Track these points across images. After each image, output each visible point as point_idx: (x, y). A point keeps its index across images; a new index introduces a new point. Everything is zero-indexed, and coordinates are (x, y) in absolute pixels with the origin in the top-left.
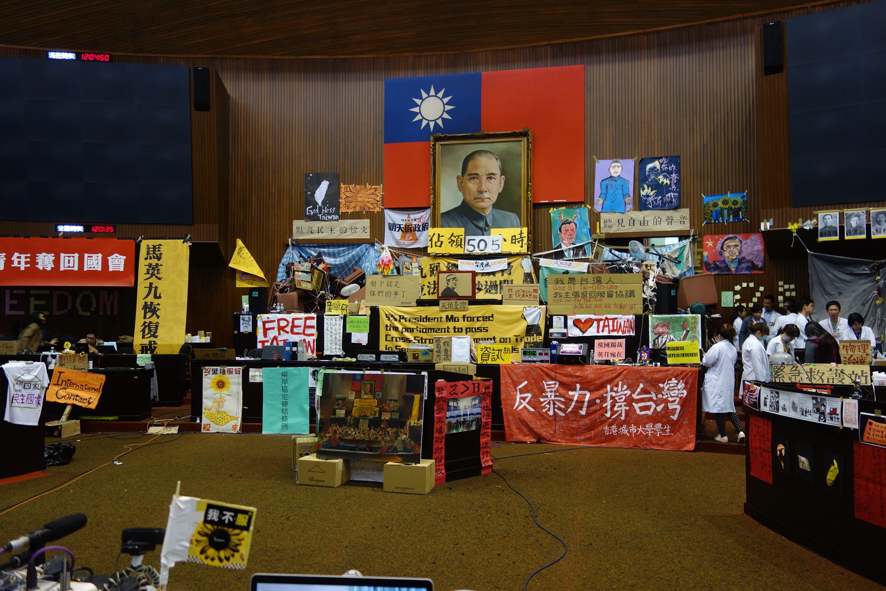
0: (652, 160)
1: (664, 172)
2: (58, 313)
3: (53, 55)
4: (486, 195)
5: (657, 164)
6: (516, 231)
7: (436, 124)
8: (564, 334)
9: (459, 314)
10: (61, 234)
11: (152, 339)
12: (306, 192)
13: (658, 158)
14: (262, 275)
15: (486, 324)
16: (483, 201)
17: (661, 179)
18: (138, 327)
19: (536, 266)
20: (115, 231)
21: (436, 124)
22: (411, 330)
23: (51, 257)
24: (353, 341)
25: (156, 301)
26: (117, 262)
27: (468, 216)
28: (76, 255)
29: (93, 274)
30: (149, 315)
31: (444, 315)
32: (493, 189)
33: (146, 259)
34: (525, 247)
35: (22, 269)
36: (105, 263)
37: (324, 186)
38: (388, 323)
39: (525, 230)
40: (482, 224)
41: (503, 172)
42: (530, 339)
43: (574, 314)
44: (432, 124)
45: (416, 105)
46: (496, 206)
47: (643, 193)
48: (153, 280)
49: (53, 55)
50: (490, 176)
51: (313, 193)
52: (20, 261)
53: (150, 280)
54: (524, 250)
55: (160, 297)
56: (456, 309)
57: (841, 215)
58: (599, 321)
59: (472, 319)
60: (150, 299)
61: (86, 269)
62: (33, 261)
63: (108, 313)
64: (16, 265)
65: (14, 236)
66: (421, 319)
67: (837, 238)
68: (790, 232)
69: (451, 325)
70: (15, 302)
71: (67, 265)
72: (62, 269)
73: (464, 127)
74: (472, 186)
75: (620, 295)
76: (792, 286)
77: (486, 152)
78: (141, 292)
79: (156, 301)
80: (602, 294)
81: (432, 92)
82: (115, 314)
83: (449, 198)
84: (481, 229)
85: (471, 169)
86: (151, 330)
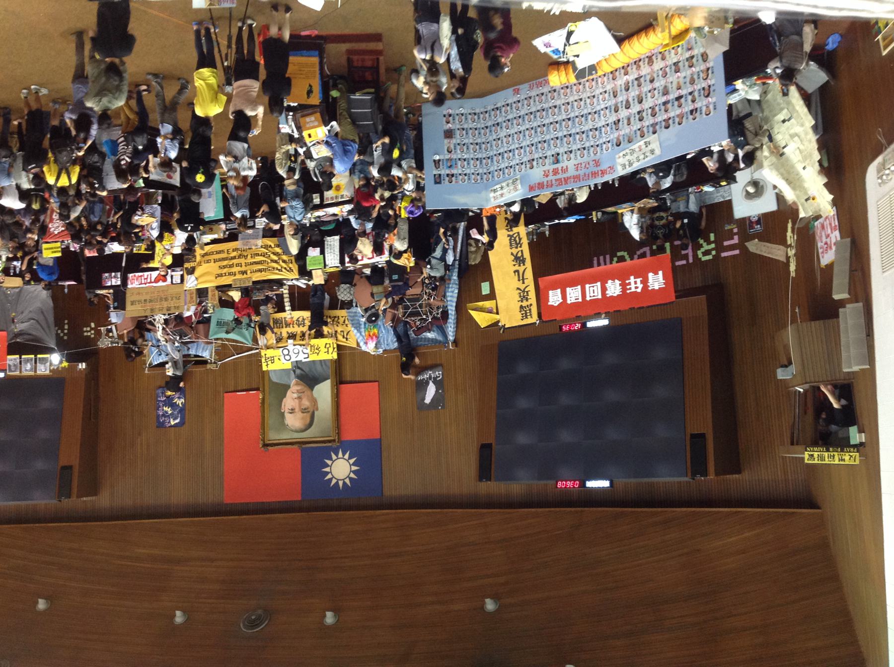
0: (176, 425)
1: (168, 416)
2: (645, 249)
3: (606, 484)
4: (295, 395)
5: (173, 423)
6: (272, 367)
7: (337, 455)
8: (173, 271)
9: (238, 276)
10: (603, 316)
11: (511, 233)
12: (443, 391)
13: (171, 426)
14: (472, 313)
15: (220, 271)
16: (298, 391)
17: (169, 410)
18: (525, 242)
19: (255, 340)
20: (561, 327)
21: (337, 455)
22: (273, 261)
23: (609, 293)
24: (318, 250)
25: (517, 268)
26: (554, 298)
27: (308, 376)
28: (588, 298)
29: (573, 284)
30: (520, 254)
31: (249, 275)
32: (290, 401)
33: (531, 305)
34: (263, 354)
35: (632, 277)
36: (564, 296)
37: (428, 400)
38: (291, 265)
39: (265, 368)
40: (298, 371)
41: (282, 415)
42: (192, 264)
43: (168, 285)
44: (340, 455)
45: (354, 472)
46: (287, 387)
47: (183, 400)
48: (522, 287)
49: (606, 484)
50: (292, 411)
51: (437, 391)
52: (635, 285)
53: (524, 286)
54: (263, 353)
55: (515, 272)
56: (240, 280)
57: (35, 371)
58: (151, 282)
59: (230, 274)
60: (521, 269)
61: (579, 287)
62: (624, 286)
63: (601, 258)
64: (639, 280)
65: (643, 307)
66: (265, 270)
67: (39, 356)
68: (67, 361)
69: (243, 268)
70: (683, 252)
71: (595, 288)
72: (599, 284)
73: (314, 455)
74: (306, 403)
75: (139, 301)
76: (85, 334)
77: (297, 431)
78: (529, 274)
79: (517, 268)
80: (151, 301)
81: (341, 483)
82: (595, 258)
83: (324, 391)
84: (299, 368)
85: (308, 416)
86: (515, 242)
